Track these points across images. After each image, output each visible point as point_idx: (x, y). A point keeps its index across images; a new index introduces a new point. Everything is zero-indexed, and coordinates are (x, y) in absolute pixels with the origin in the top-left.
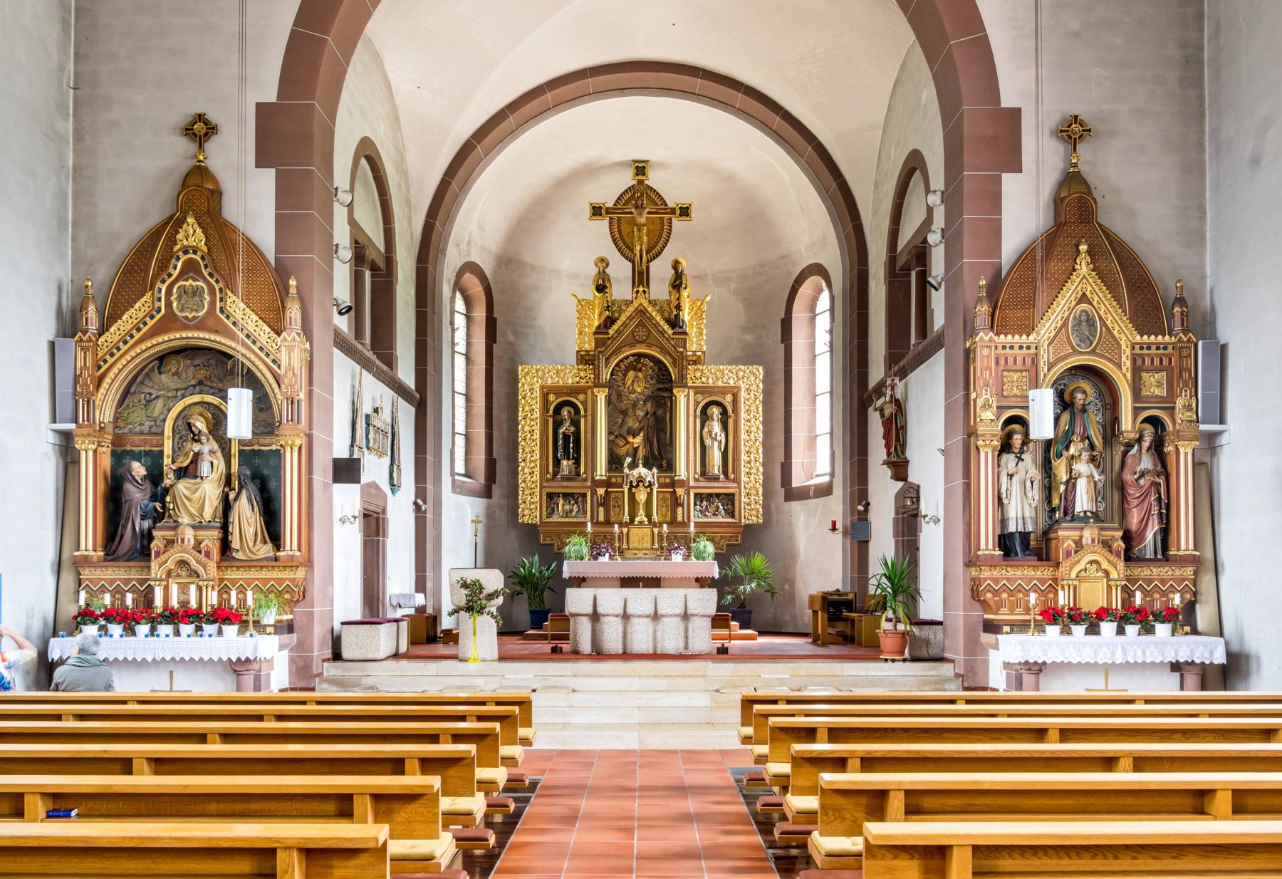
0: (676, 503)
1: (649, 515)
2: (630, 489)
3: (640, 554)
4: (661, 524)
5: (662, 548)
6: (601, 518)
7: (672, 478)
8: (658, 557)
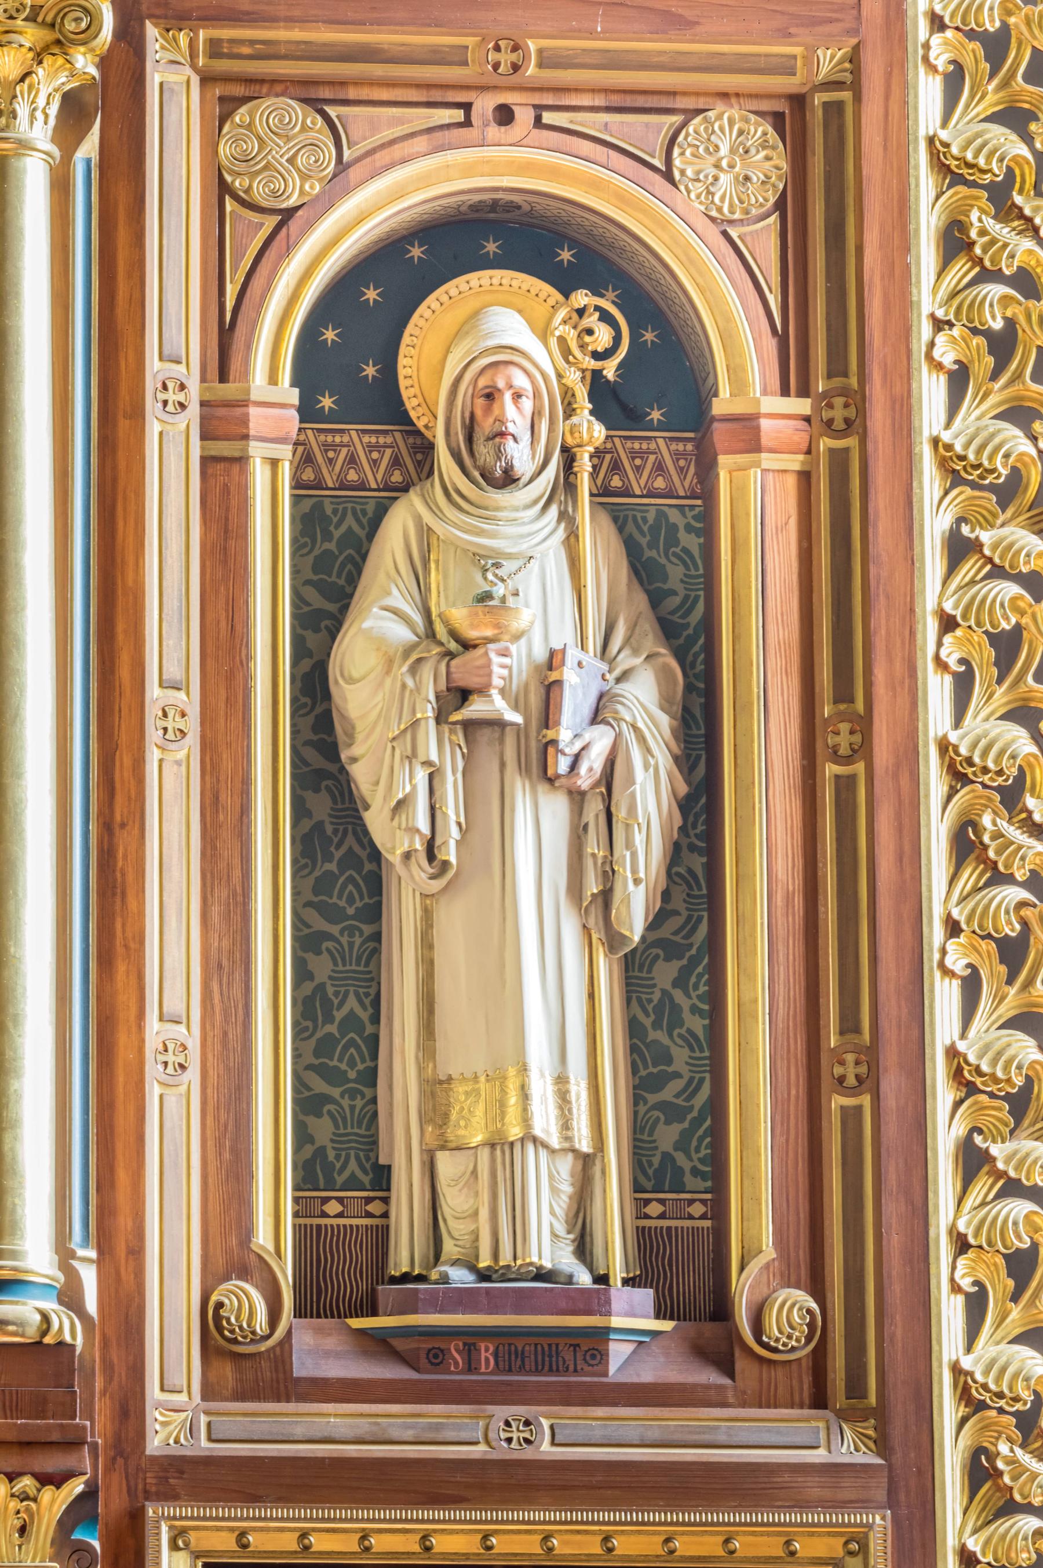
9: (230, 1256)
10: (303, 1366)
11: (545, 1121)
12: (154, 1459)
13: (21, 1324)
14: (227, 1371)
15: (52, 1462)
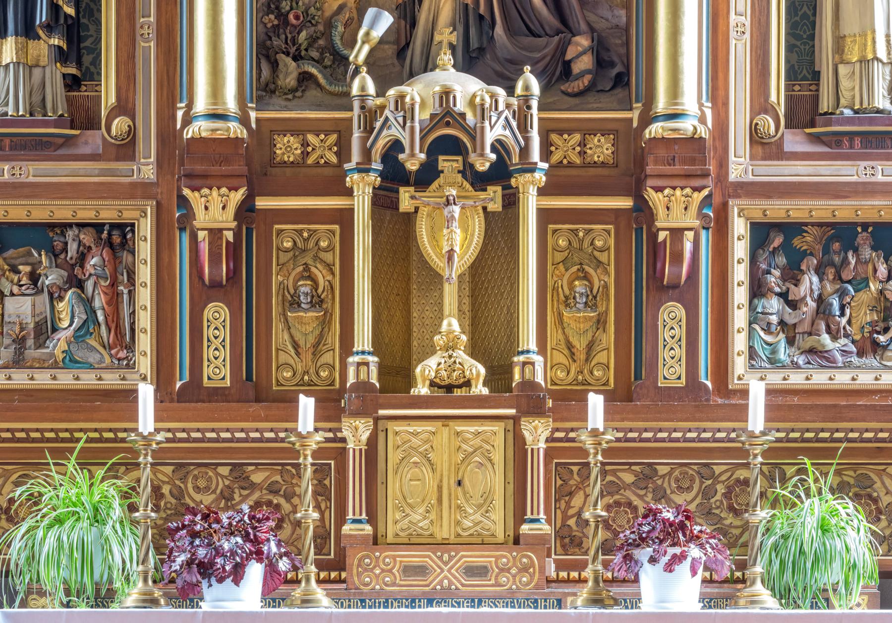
0: (649, 270)
1: (492, 342)
2: (384, 201)
3: (446, 572)
4: (570, 401)
5: (569, 540)
6: (218, 369)
7: (628, 138)
8: (551, 591)
9: (760, 104)
10: (788, 147)
11: (882, 53)
12: (732, 183)
13: (685, 130)
14: (759, 150)
15: (697, 183)
